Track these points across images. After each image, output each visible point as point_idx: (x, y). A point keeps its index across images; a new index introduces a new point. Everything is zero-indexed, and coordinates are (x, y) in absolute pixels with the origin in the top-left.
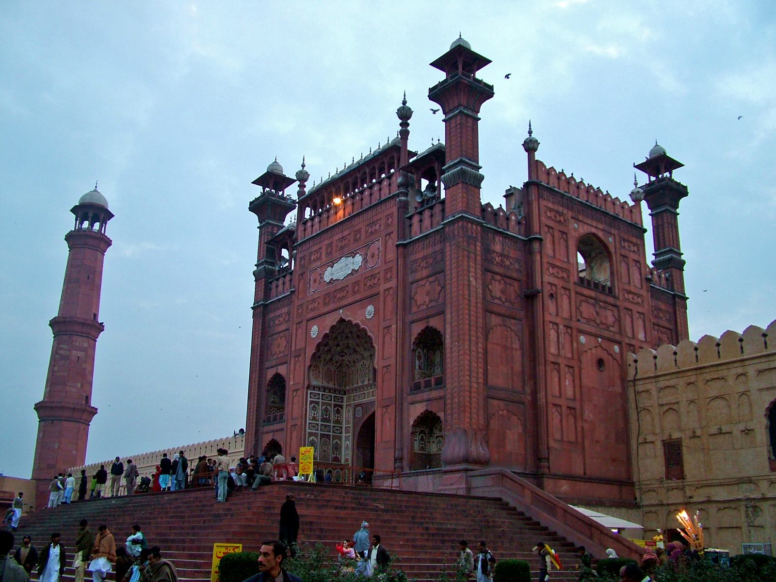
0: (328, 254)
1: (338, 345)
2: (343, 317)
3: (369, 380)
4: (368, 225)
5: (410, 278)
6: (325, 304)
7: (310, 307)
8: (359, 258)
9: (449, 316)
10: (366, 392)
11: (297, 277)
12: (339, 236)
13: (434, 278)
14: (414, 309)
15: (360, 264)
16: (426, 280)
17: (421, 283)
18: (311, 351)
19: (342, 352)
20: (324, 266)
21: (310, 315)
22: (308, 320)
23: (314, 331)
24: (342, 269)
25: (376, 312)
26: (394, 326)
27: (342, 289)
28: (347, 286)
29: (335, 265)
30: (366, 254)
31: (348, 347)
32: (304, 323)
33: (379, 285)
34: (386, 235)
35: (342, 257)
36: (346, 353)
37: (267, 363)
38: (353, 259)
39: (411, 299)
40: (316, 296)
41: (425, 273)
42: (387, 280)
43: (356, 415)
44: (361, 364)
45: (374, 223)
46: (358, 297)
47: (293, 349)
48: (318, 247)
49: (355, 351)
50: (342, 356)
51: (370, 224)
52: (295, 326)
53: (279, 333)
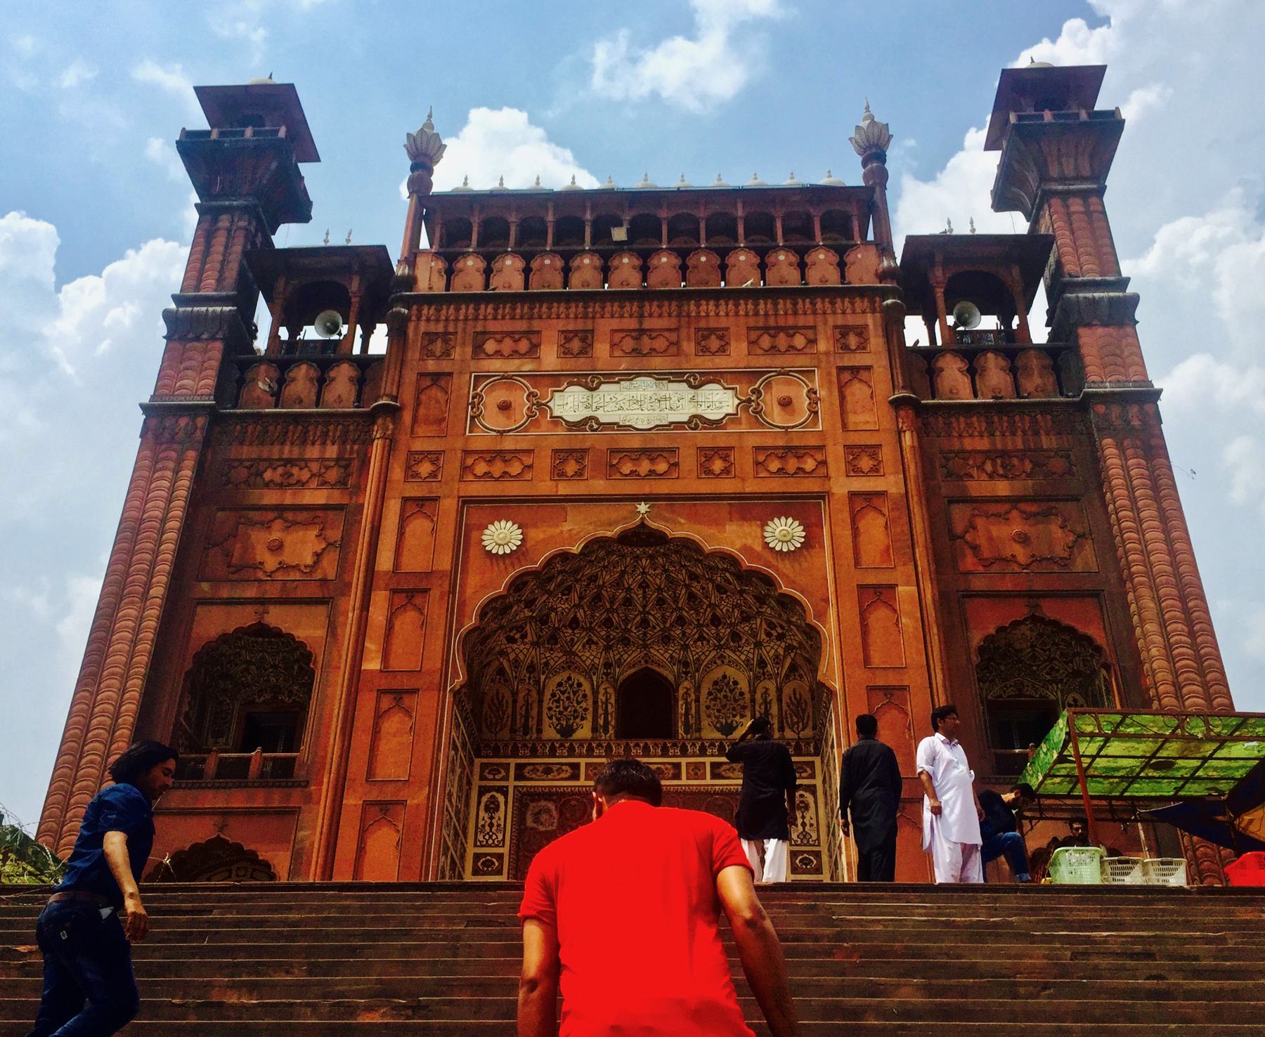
0: (565, 352)
1: (530, 604)
2: (654, 525)
3: (594, 729)
4: (757, 328)
5: (946, 489)
6: (558, 473)
7: (481, 468)
8: (718, 401)
9: (1152, 605)
10: (583, 762)
11: (410, 377)
12: (632, 324)
13: (1044, 506)
14: (969, 562)
15: (731, 410)
16: (1007, 507)
17: (993, 508)
18: (481, 588)
19: (520, 629)
20: (556, 380)
21: (476, 489)
22: (466, 501)
23: (502, 535)
24: (640, 404)
25: (811, 542)
26: (905, 591)
27: (650, 453)
28: (672, 451)
29: (603, 387)
30: (757, 392)
31: (544, 620)
32: (449, 505)
33: (827, 477)
34: (841, 369)
35: (639, 375)
36: (524, 636)
37: (205, 586)
38: (692, 392)
39: (954, 537)
40: (508, 445)
41: (1002, 488)
42: (853, 470)
43: (530, 822)
44: (558, 679)
45: (791, 331)
46: (727, 486)
47: (385, 562)
48: (521, 326)
49: (553, 639)
50: (511, 640)
51: (766, 329)
52: (393, 508)
53: (280, 509)
